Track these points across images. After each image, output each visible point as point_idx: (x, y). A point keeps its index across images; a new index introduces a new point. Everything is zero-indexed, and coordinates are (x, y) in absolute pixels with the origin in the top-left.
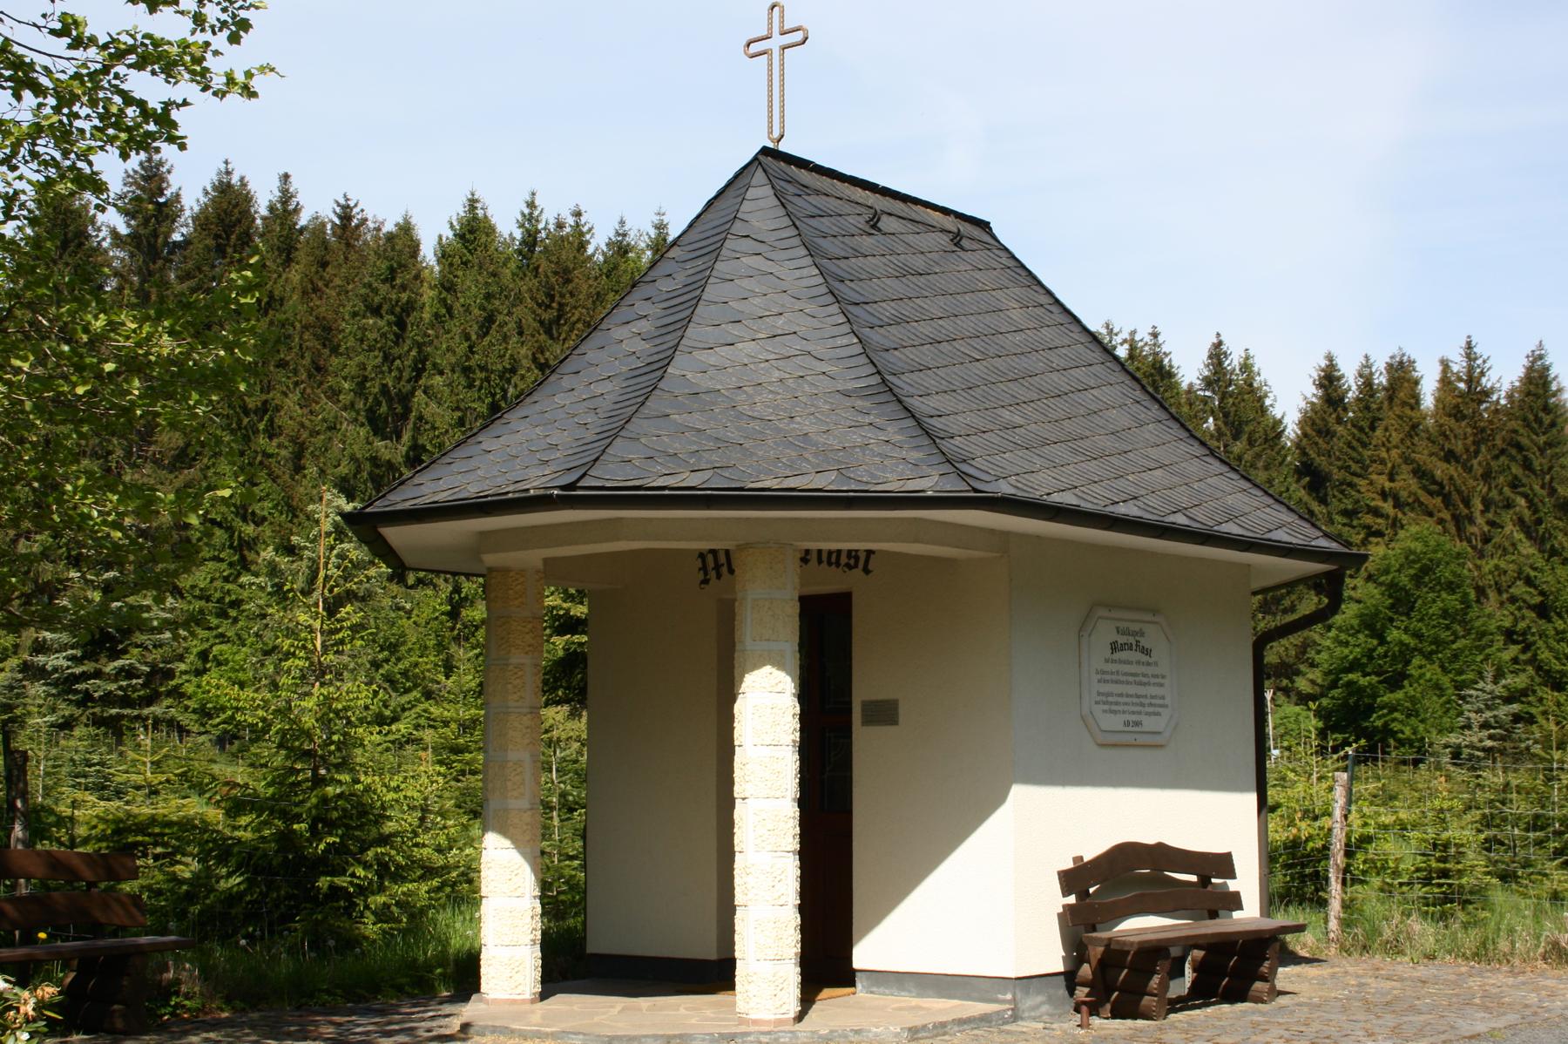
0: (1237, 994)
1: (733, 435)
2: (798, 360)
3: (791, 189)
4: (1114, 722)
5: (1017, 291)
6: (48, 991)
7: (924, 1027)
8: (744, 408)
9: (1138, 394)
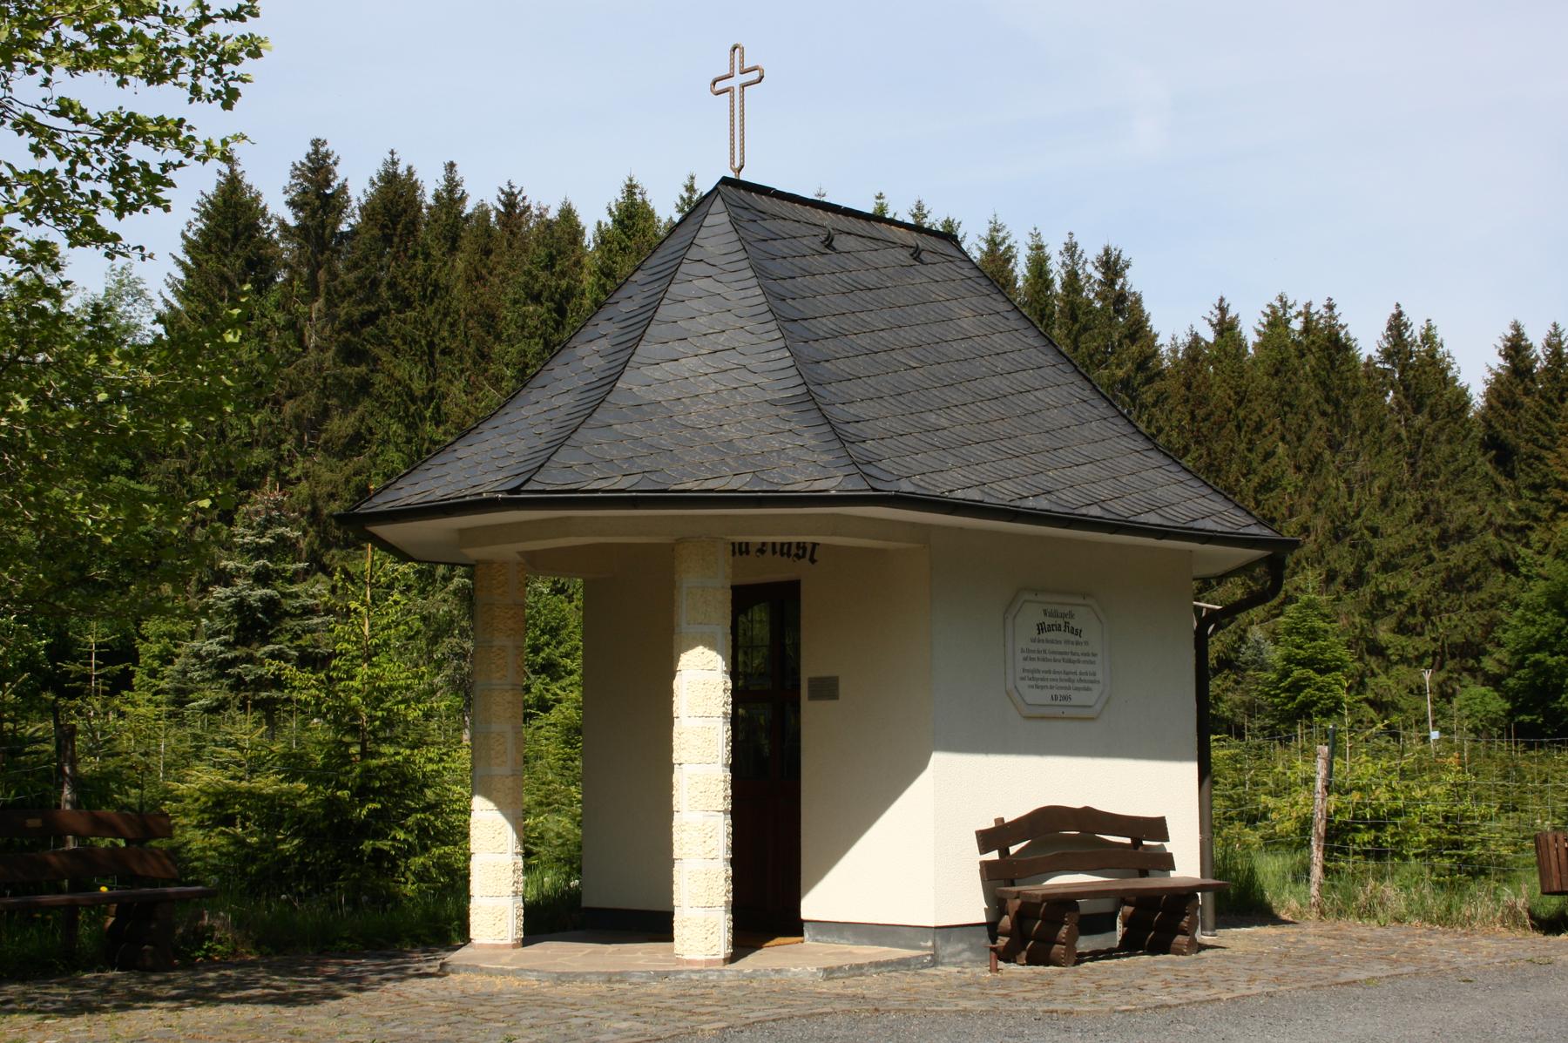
1: (666, 442)
2: (733, 374)
3: (746, 215)
4: (1043, 697)
5: (974, 300)
7: (840, 968)
8: (680, 419)
9: (1087, 393)
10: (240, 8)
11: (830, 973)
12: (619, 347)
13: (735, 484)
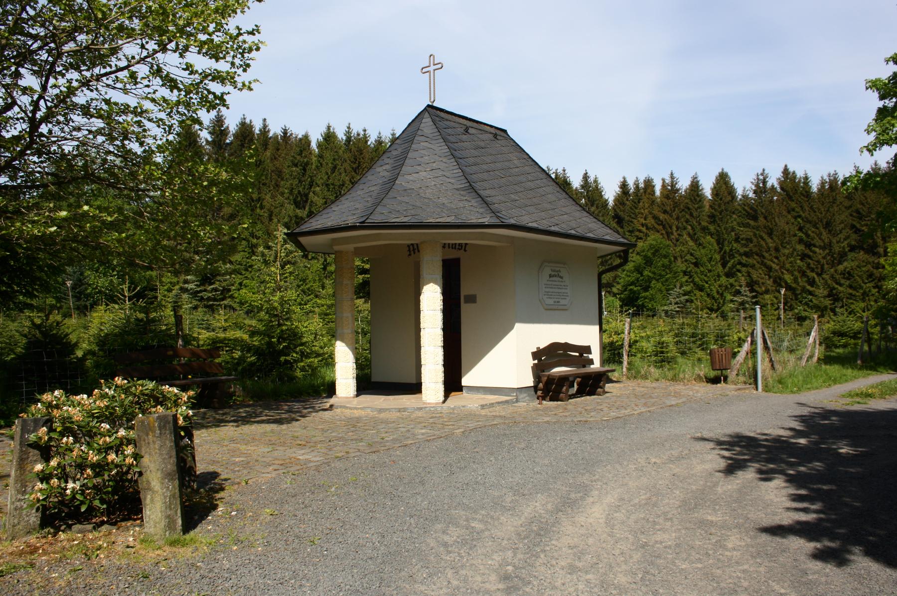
0: (592, 393)
1: (418, 204)
2: (441, 178)
3: (437, 119)
4: (551, 302)
6: (191, 393)
7: (486, 405)
8: (423, 195)
9: (558, 189)
10: (253, 30)
11: (483, 407)
12: (394, 168)
13: (449, 220)
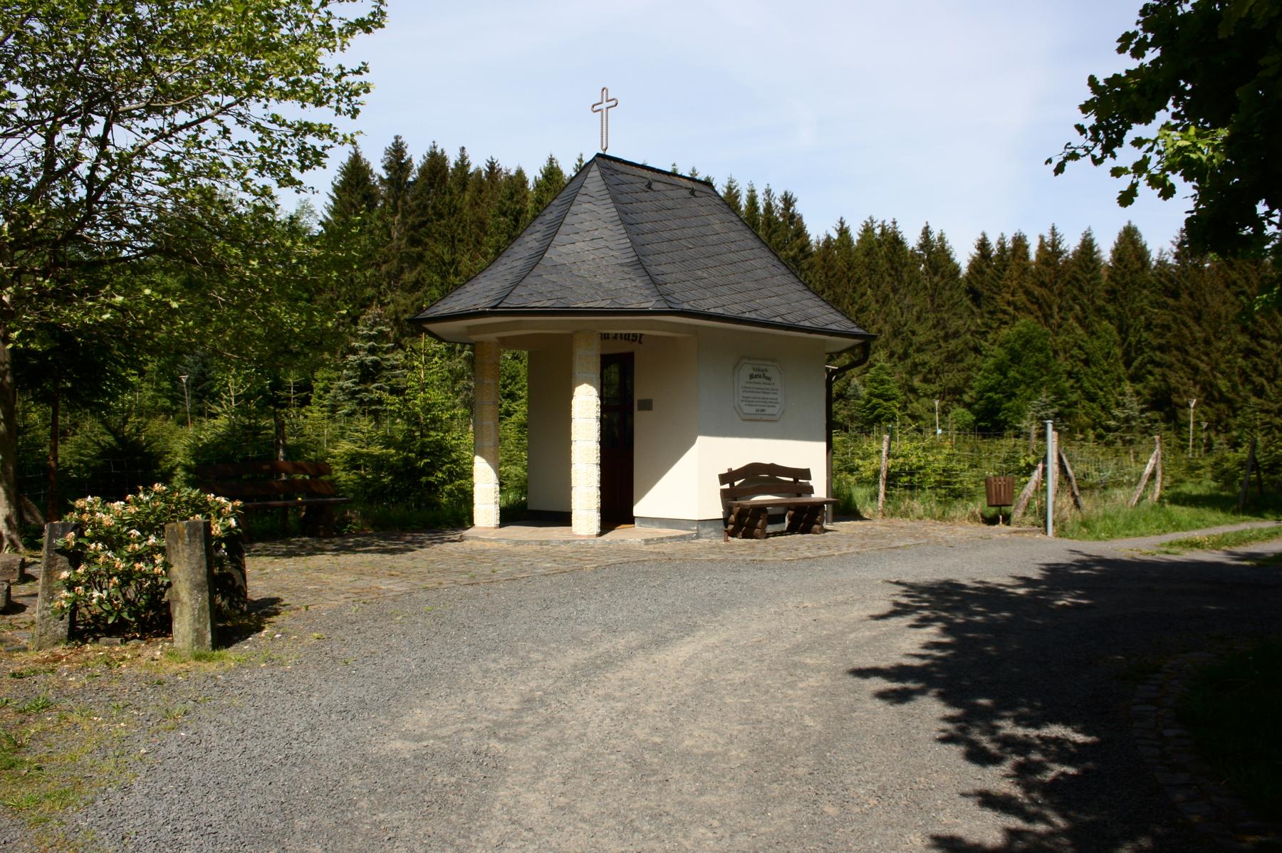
0: (806, 530)
1: (568, 284)
2: (602, 250)
3: (609, 172)
4: (752, 410)
5: (721, 215)
6: (238, 503)
8: (576, 273)
9: (776, 262)
10: (360, 68)
11: (647, 541)
12: (545, 237)
13: (603, 304)
